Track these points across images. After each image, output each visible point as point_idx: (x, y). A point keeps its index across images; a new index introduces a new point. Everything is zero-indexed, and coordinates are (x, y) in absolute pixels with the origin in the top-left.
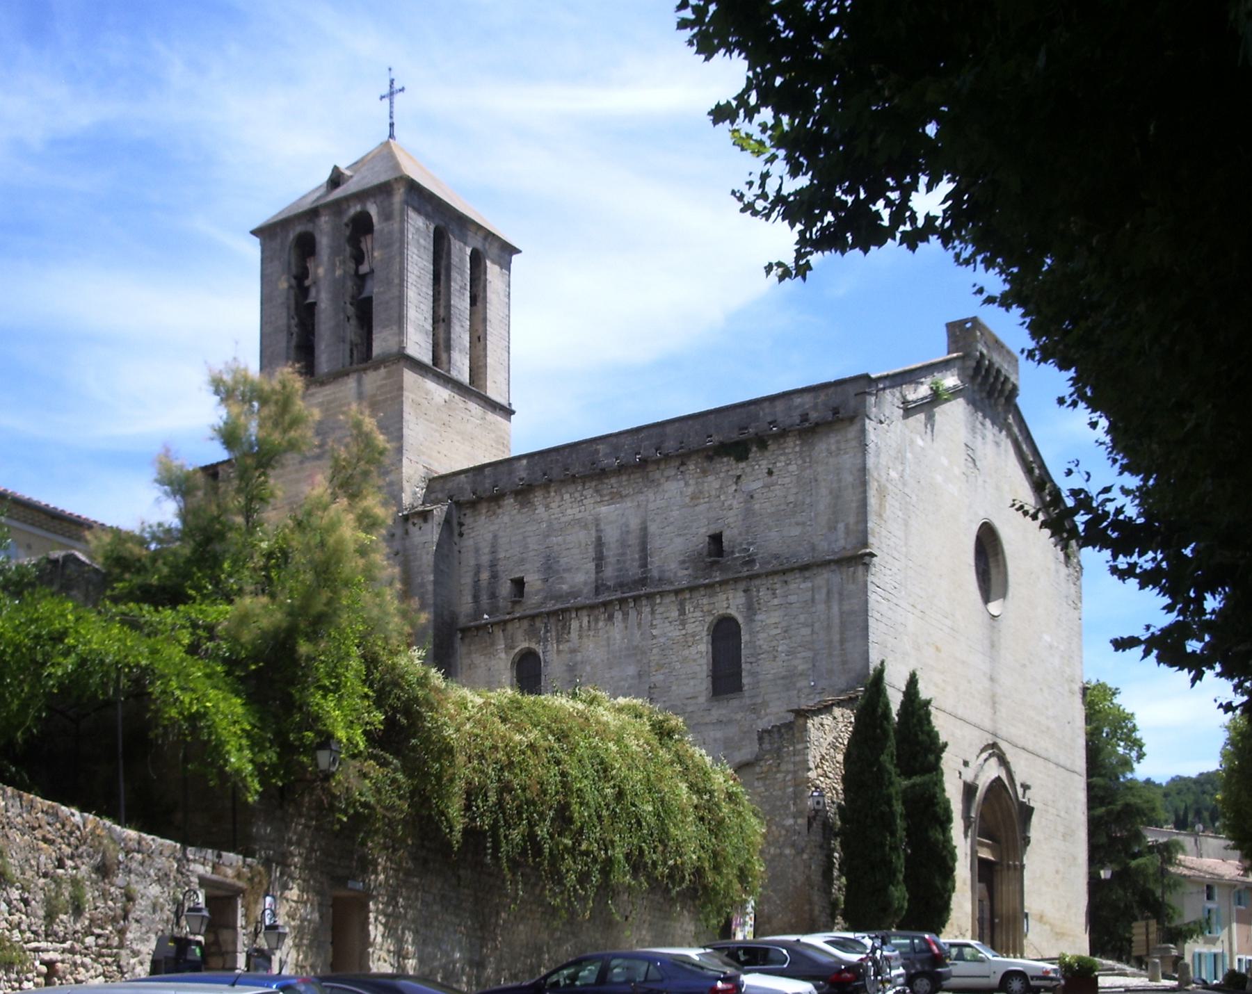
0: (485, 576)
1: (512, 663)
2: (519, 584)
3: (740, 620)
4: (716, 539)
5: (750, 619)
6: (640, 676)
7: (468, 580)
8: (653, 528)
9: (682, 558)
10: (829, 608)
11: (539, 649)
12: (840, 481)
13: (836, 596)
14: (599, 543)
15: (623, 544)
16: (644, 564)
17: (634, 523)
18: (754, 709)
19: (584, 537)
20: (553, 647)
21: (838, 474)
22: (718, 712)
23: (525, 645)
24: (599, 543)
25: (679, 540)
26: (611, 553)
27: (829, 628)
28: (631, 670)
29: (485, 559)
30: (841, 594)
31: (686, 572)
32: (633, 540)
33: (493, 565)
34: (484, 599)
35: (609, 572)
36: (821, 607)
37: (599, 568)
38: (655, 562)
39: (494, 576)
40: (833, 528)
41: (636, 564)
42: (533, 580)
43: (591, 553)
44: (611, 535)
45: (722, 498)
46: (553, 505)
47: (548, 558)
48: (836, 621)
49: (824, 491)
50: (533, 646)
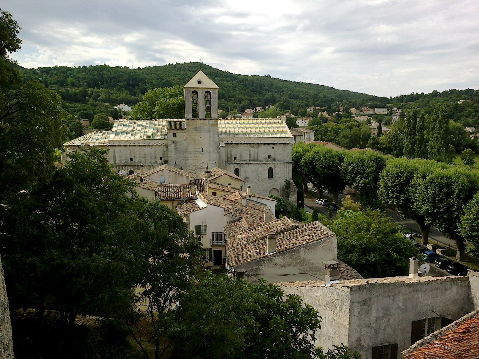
0: (229, 155)
2: (235, 158)
3: (273, 168)
4: (269, 157)
5: (275, 169)
6: (257, 175)
11: (239, 168)
14: (250, 154)
15: (254, 154)
16: (258, 157)
17: (256, 152)
18: (275, 181)
22: (271, 180)
24: (250, 154)
26: (252, 155)
27: (287, 171)
28: (256, 174)
29: (229, 153)
32: (256, 154)
33: (231, 154)
34: (229, 159)
35: (252, 158)
36: (286, 168)
37: (250, 158)
38: (259, 158)
39: (231, 156)
40: (287, 158)
42: (238, 158)
43: (249, 155)
44: (252, 153)
47: (241, 154)
48: (288, 170)
50: (238, 168)
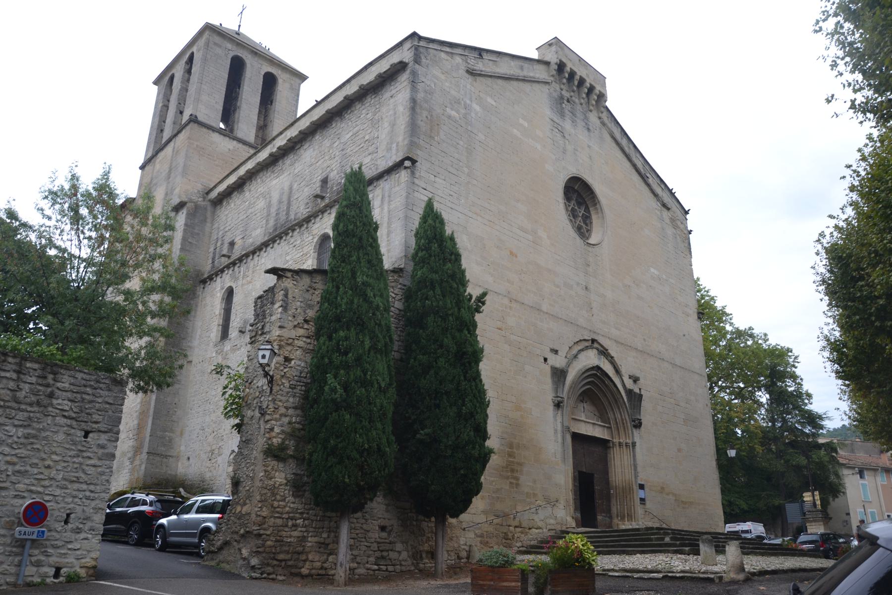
0: (219, 244)
1: (223, 299)
2: (232, 244)
7: (212, 249)
8: (295, 186)
9: (307, 201)
10: (382, 209)
12: (395, 114)
13: (387, 199)
14: (269, 205)
15: (280, 202)
19: (261, 204)
20: (240, 282)
21: (394, 109)
23: (229, 285)
25: (306, 189)
30: (389, 196)
31: (308, 210)
32: (285, 198)
41: (284, 213)
42: (239, 242)
45: (331, 152)
46: (252, 189)
49: (386, 125)
